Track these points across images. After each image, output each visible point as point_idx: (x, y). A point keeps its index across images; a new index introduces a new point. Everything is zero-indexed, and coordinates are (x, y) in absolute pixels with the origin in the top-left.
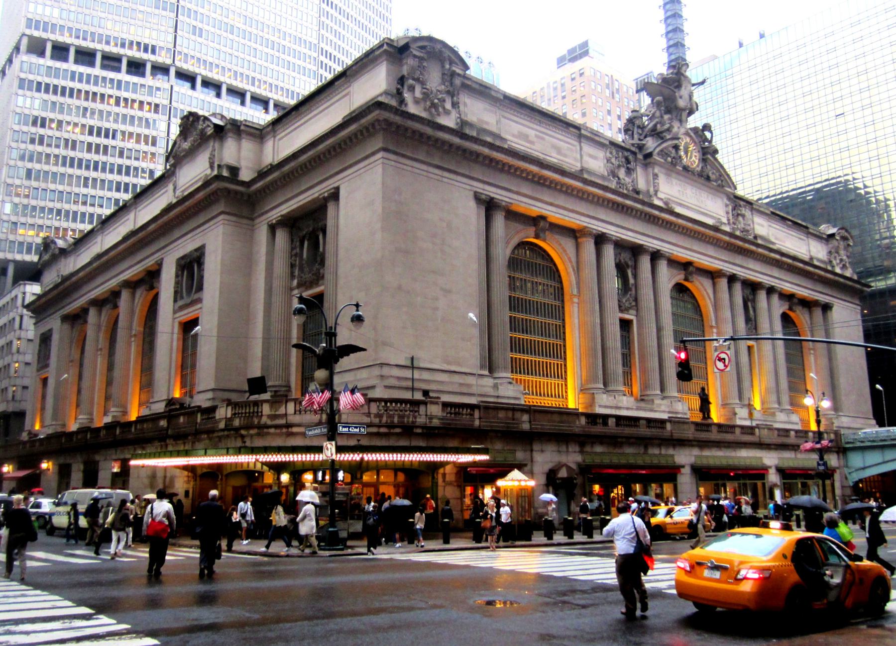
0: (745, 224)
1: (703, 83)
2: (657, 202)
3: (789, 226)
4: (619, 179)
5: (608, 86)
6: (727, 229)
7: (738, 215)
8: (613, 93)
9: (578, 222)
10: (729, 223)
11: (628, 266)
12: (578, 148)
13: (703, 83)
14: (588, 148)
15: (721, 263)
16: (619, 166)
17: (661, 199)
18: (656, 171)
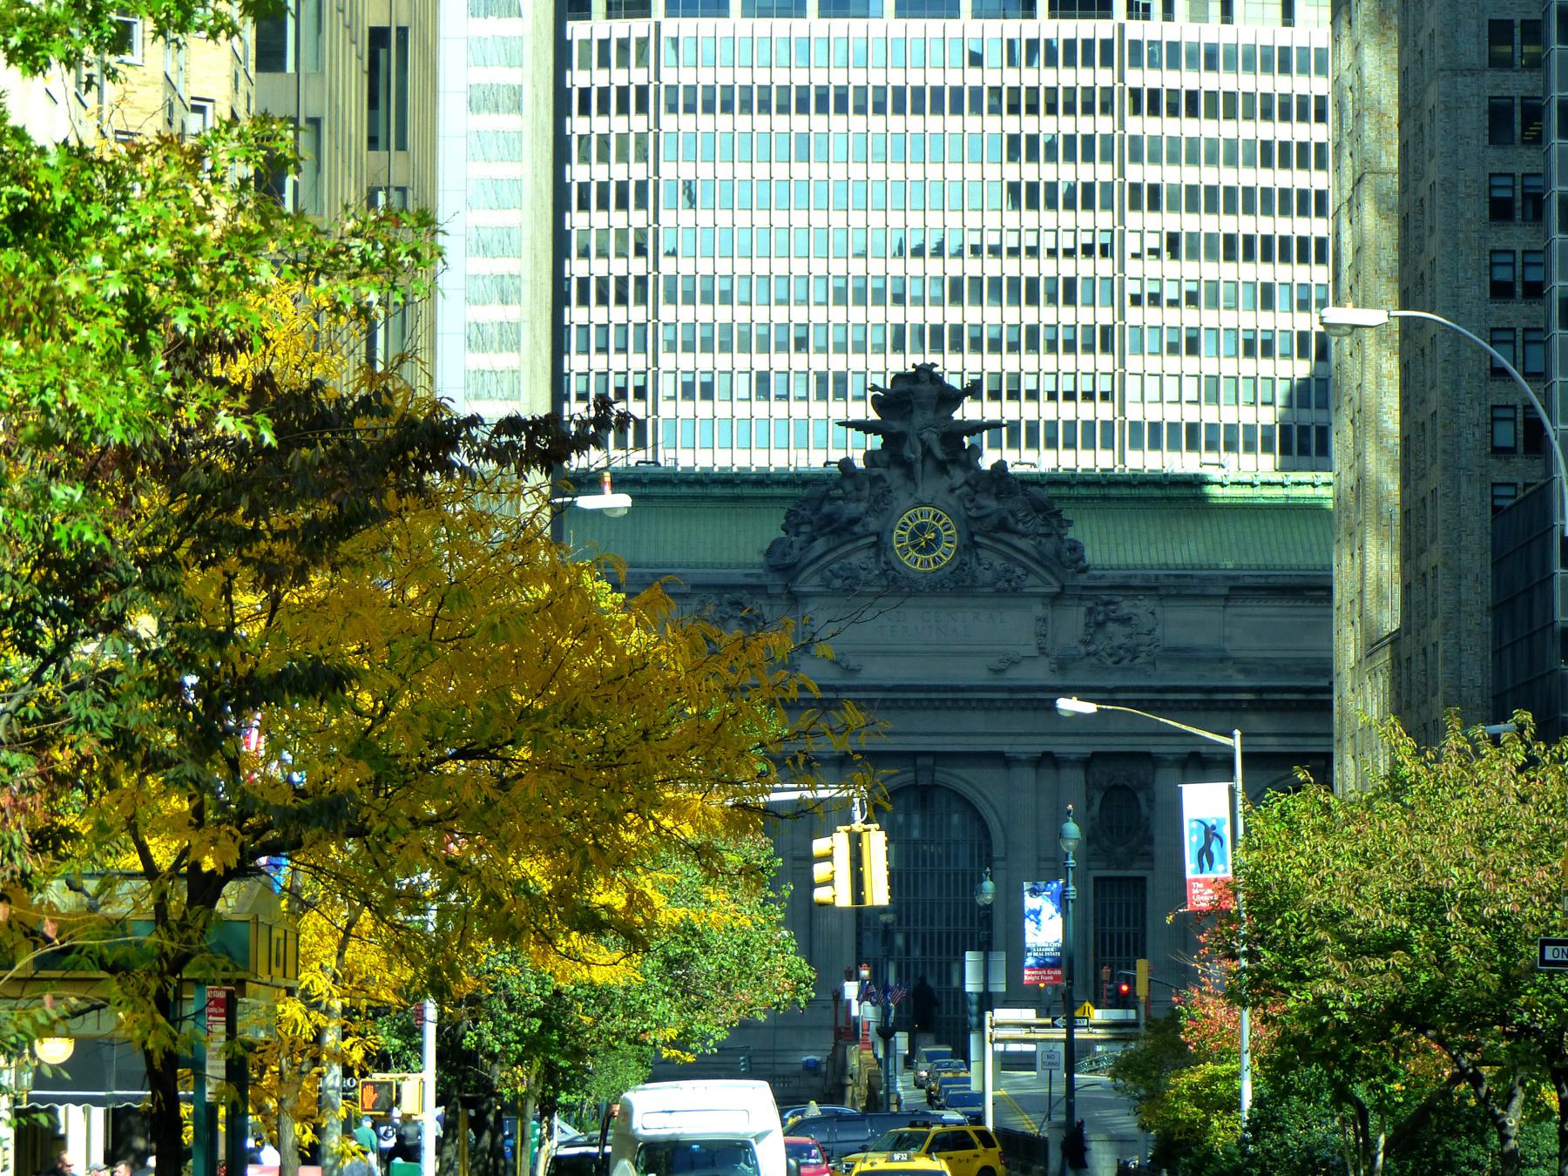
10: (1047, 655)
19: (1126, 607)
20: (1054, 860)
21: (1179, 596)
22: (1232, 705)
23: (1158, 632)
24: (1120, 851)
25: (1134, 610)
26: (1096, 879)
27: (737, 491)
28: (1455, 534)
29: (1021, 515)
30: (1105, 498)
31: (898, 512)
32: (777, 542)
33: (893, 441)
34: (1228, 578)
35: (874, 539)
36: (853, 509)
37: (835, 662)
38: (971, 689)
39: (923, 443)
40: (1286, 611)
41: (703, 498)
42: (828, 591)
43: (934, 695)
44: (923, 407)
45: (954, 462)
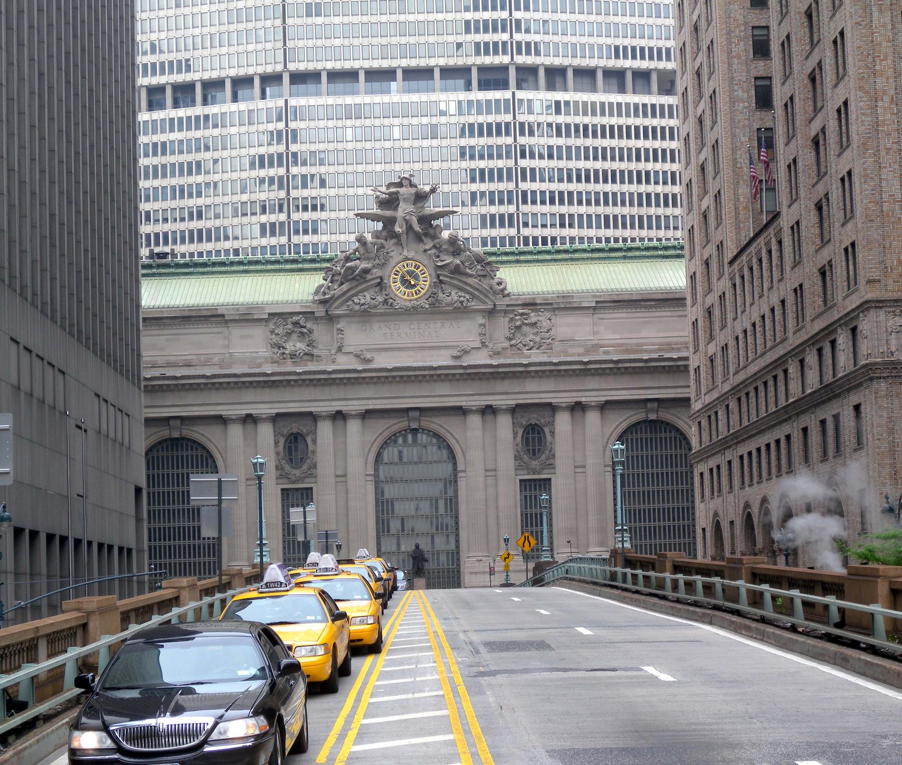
4: (284, 348)
10: (487, 346)
13: (433, 191)
14: (236, 332)
15: (463, 398)
16: (289, 334)
19: (533, 317)
20: (495, 470)
21: (566, 309)
22: (600, 371)
23: (552, 332)
24: (535, 464)
26: (520, 480)
27: (300, 266)
28: (870, 59)
29: (467, 264)
30: (518, 262)
32: (322, 286)
33: (389, 223)
34: (595, 296)
35: (379, 280)
36: (364, 265)
37: (357, 356)
38: (440, 368)
39: (407, 222)
40: (630, 315)
41: (280, 271)
42: (352, 315)
44: (405, 200)
45: (426, 235)
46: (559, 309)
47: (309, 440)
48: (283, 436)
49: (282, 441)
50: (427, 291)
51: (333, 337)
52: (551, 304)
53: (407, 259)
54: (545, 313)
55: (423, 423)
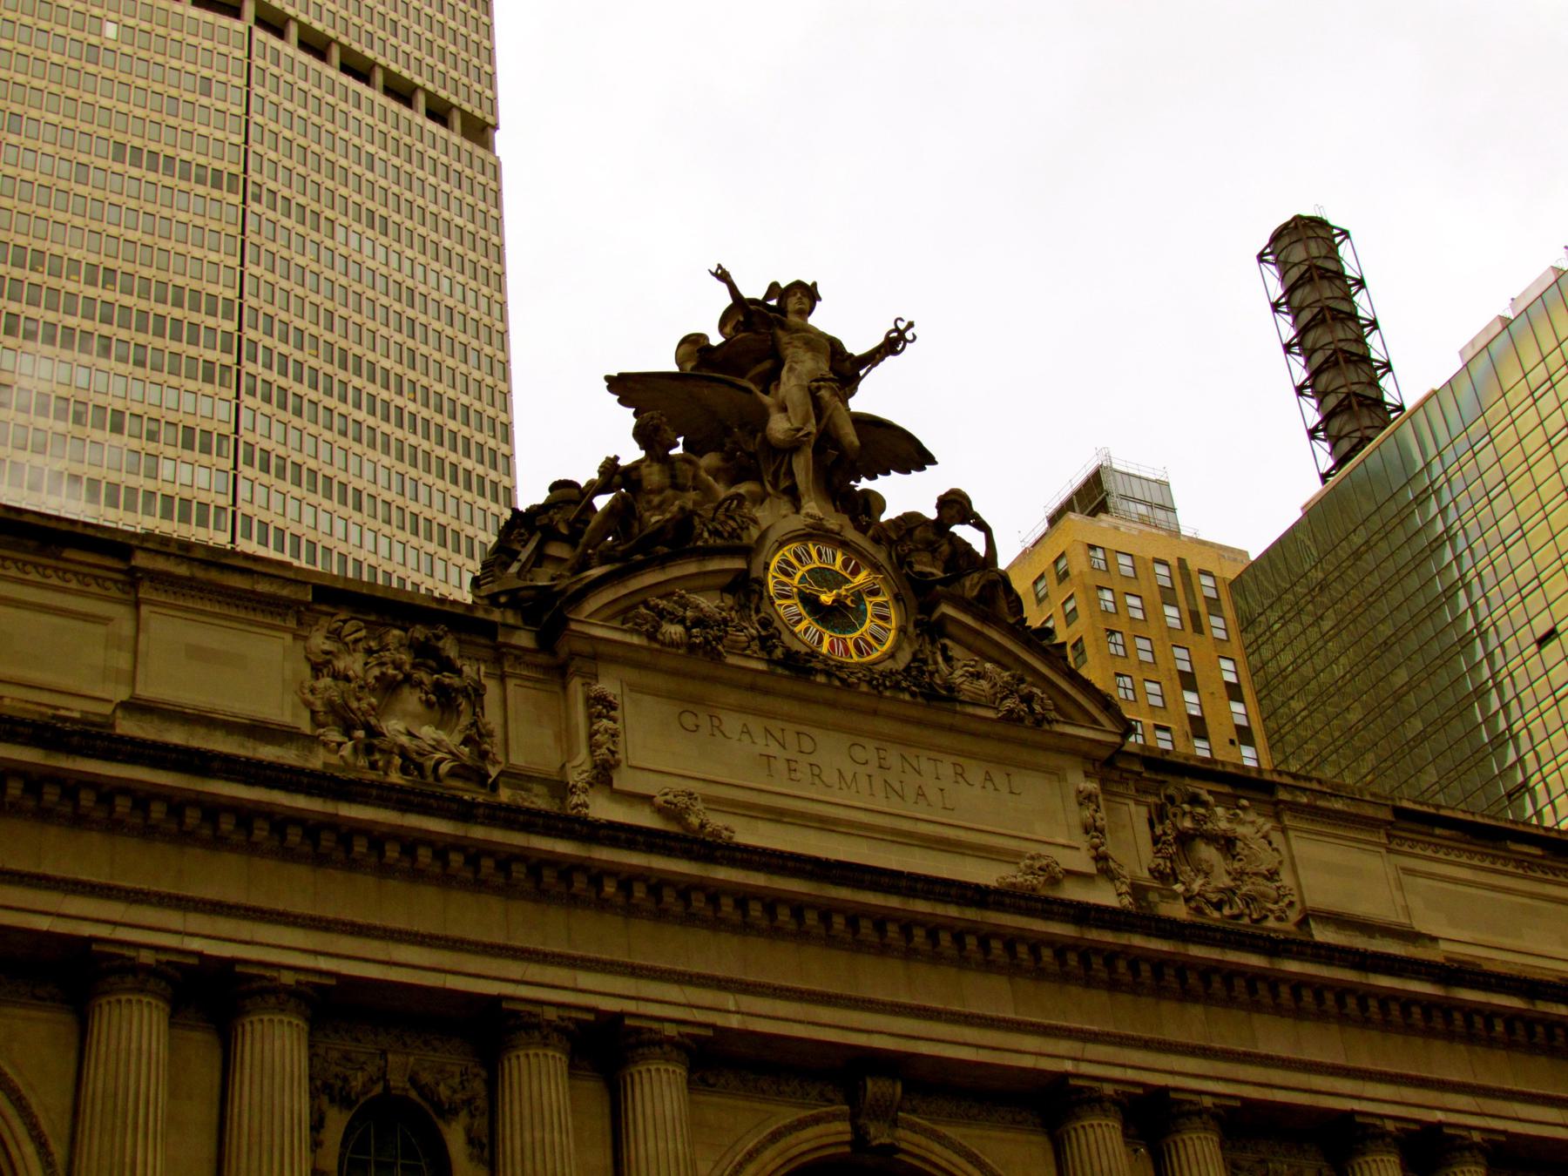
0: (1239, 875)
1: (893, 344)
2: (603, 809)
3: (1522, 862)
4: (373, 732)
5: (1168, 596)
6: (1105, 896)
7: (1185, 840)
8: (1195, 617)
9: (43, 924)
11: (448, 1113)
12: (127, 628)
13: (893, 344)
15: (1063, 1047)
16: (389, 688)
17: (647, 799)
18: (608, 686)
23: (1286, 879)
25: (1241, 830)
31: (773, 536)
35: (738, 564)
43: (921, 906)
46: (1295, 808)
47: (455, 1138)
48: (344, 1101)
49: (337, 1121)
50: (897, 647)
51: (565, 736)
52: (1268, 788)
53: (817, 533)
54: (1251, 816)
55: (907, 1139)
